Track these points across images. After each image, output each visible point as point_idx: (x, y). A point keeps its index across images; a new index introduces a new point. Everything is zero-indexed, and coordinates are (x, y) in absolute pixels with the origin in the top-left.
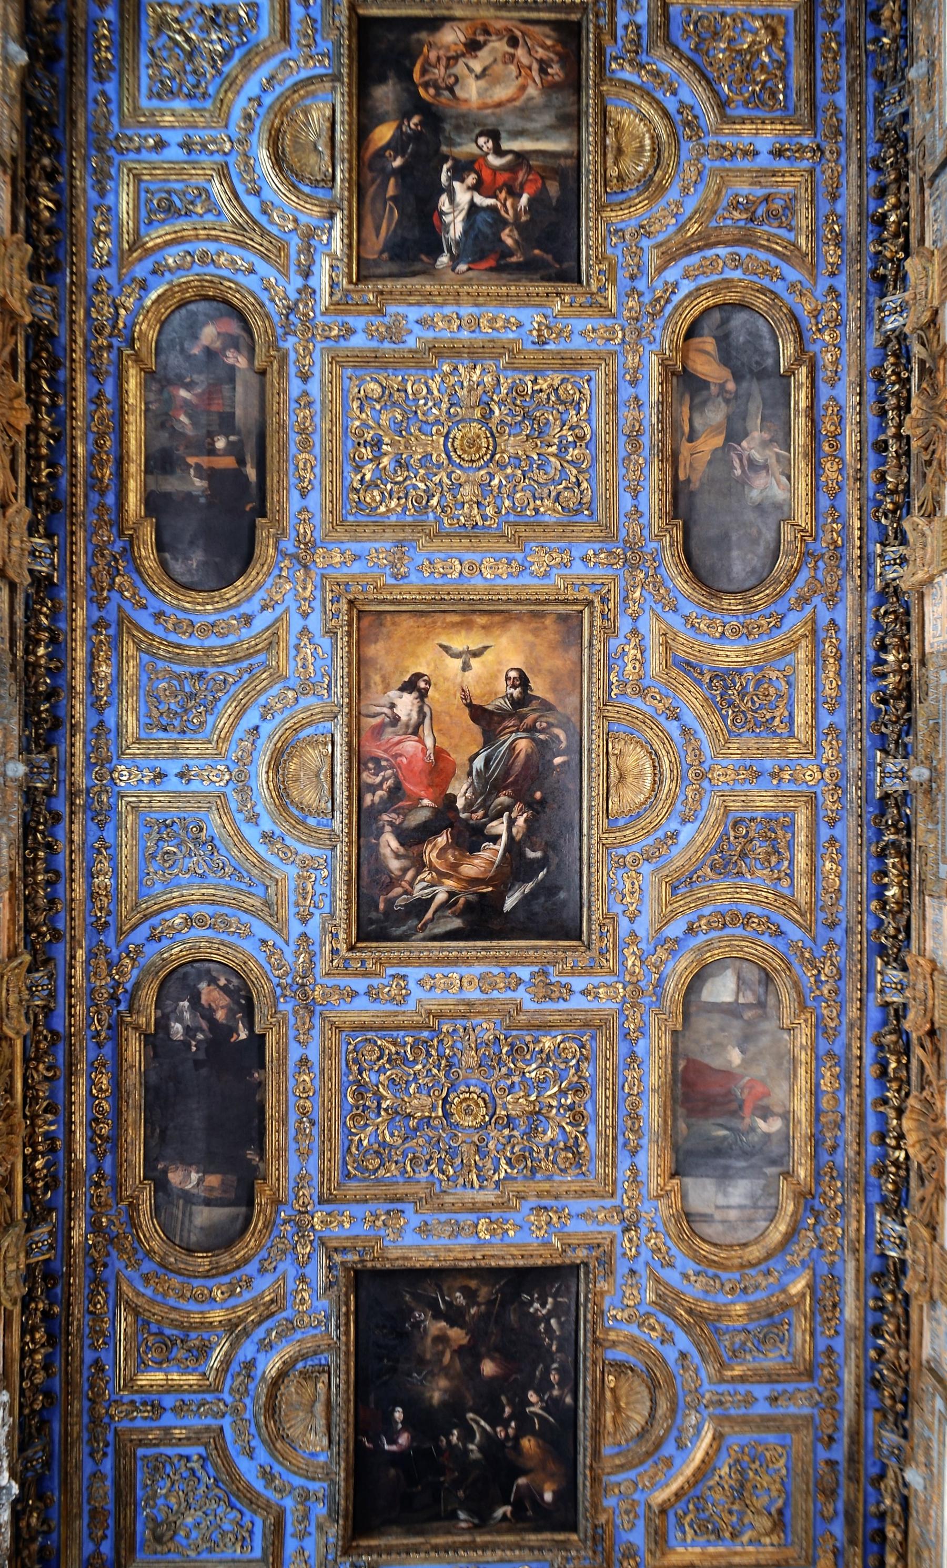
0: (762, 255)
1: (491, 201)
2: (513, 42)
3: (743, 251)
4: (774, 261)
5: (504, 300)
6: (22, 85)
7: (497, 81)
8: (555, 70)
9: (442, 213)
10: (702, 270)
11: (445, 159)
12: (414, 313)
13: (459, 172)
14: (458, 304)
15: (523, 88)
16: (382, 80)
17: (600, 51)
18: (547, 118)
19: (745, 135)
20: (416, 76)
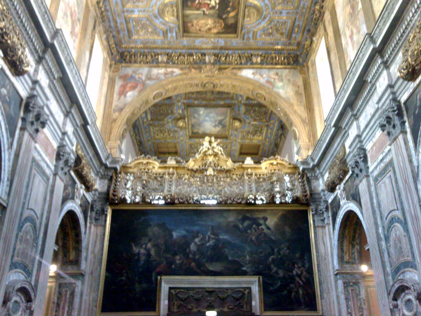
2: (200, 30)
6: (316, 32)
8: (189, 25)
11: (217, 10)
13: (213, 8)
15: (198, 22)
16: (232, 25)
17: (179, 28)
18: (191, 17)
19: (142, 15)
20: (223, 25)
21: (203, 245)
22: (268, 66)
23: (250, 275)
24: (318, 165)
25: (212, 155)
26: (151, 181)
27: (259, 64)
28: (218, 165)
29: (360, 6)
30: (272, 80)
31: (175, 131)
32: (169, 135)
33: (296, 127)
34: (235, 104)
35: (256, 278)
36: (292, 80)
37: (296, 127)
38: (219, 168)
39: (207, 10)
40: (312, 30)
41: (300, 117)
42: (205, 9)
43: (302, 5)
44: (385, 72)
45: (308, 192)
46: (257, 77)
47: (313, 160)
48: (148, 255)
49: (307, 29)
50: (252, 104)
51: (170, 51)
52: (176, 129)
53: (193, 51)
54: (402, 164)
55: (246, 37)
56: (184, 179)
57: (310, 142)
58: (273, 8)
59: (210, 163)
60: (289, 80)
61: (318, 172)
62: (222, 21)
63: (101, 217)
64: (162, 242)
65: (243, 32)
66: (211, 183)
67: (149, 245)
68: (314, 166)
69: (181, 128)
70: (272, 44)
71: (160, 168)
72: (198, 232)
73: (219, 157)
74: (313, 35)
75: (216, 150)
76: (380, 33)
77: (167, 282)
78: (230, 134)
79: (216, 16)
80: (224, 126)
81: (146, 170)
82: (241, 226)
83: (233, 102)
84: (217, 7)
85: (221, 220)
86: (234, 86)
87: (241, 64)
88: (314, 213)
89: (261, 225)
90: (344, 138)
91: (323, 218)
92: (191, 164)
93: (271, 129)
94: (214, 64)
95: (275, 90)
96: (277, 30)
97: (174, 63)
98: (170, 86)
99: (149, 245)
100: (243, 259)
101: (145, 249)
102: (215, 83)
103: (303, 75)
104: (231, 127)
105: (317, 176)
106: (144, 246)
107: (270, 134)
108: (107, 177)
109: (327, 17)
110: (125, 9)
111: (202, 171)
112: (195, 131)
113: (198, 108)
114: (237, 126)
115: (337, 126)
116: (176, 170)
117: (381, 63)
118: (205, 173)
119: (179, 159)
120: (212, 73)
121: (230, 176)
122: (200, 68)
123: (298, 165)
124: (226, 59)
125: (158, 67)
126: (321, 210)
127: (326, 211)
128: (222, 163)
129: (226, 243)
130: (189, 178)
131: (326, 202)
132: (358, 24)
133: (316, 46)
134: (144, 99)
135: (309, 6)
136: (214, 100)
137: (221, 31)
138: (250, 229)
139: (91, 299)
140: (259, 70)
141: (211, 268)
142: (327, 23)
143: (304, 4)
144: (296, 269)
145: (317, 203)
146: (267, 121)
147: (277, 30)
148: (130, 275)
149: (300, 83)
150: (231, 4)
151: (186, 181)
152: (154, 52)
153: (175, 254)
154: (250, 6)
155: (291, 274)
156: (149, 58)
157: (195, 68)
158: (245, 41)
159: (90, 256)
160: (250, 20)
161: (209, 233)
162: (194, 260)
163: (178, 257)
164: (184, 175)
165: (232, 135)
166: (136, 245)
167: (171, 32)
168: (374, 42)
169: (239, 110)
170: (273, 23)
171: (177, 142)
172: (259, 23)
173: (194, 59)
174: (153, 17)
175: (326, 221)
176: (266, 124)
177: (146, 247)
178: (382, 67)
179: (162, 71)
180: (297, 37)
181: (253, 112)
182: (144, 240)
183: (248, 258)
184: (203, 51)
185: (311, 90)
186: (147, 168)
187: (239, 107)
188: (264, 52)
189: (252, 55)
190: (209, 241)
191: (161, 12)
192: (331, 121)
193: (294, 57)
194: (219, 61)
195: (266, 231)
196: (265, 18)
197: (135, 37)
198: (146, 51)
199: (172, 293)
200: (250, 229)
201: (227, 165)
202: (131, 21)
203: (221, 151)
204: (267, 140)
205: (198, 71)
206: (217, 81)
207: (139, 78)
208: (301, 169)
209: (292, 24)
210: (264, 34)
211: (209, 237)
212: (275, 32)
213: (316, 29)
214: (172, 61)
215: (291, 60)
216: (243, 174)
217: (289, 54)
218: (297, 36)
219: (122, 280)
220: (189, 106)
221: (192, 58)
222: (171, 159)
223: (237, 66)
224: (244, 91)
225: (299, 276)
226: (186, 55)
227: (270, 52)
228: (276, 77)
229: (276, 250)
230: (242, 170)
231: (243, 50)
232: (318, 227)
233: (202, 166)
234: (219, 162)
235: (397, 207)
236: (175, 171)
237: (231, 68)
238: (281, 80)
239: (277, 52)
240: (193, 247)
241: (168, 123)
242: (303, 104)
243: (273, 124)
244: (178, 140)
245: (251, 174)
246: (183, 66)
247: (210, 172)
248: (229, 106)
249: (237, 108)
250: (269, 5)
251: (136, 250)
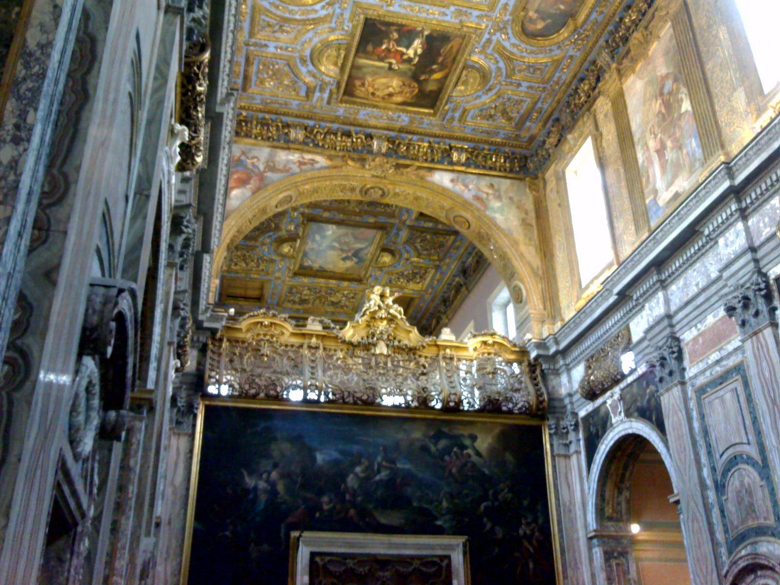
0: (279, 13)
1: (400, 49)
2: (373, 94)
3: (287, 15)
4: (273, 10)
5: (405, 17)
6: (573, 127)
7: (383, 84)
8: (358, 83)
9: (422, 48)
10: (308, 12)
11: (414, 65)
12: (448, 18)
13: (410, 60)
14: (426, 18)
15: (373, 81)
16: (431, 92)
18: (365, 70)
20: (417, 91)
21: (368, 478)
22: (477, 171)
23: (448, 534)
24: (564, 352)
25: (385, 318)
26: (277, 358)
27: (463, 165)
28: (395, 338)
29: (686, 106)
30: (485, 196)
31: (272, 261)
32: (258, 266)
33: (522, 281)
34: (393, 225)
35: (460, 540)
36: (515, 199)
37: (522, 281)
38: (396, 343)
39: (397, 63)
40: (565, 119)
41: (530, 265)
42: (394, 61)
43: (555, 79)
44: (740, 225)
45: (546, 397)
46: (459, 188)
47: (557, 342)
48: (273, 492)
49: (553, 117)
50: (423, 227)
51: (311, 123)
52: (274, 257)
53: (352, 129)
54: (767, 374)
55: (447, 117)
56: (335, 358)
57: (545, 309)
58: (508, 76)
59: (381, 333)
60: (511, 199)
61: (561, 362)
62: (416, 85)
63: (186, 420)
64: (298, 471)
65: (447, 107)
66: (383, 368)
67: (274, 475)
68: (557, 353)
69: (284, 256)
70: (488, 133)
71: (294, 334)
72: (361, 455)
73: (397, 324)
74: (570, 128)
75: (392, 311)
76: (746, 165)
77: (307, 544)
78: (367, 276)
79: (410, 74)
80: (361, 260)
81: (268, 337)
82: (433, 448)
83: (392, 221)
84: (417, 59)
85: (401, 436)
86: (417, 198)
87: (433, 161)
88: (552, 431)
89: (466, 447)
90: (631, 314)
91: (568, 442)
92: (348, 333)
93: (442, 273)
94: (385, 155)
95: (487, 213)
96: (504, 113)
97: (317, 145)
98: (307, 187)
99: (274, 475)
100: (437, 506)
101: (267, 481)
102: (386, 190)
103: (534, 193)
104: (373, 264)
105: (558, 370)
106: (264, 476)
107: (438, 281)
108: (196, 345)
109: (603, 106)
110: (253, 40)
111: (367, 347)
112: (306, 264)
113: (324, 225)
114: (384, 263)
115: (624, 296)
116: (322, 341)
117: (736, 211)
118: (373, 351)
119: (327, 321)
120: (383, 171)
121: (415, 358)
122: (363, 160)
123: (529, 349)
124: (408, 148)
125: (289, 149)
126: (564, 428)
127: (574, 430)
128: (401, 335)
129: (408, 477)
130: (344, 358)
131: (575, 414)
132: (678, 134)
133: (571, 150)
134: (261, 207)
135: (567, 81)
136: (358, 214)
137: (409, 101)
138: (449, 454)
139: (169, 573)
140: (462, 176)
142: (600, 117)
143: (560, 78)
145: (557, 415)
146: (438, 260)
147: (504, 113)
148: (239, 528)
149: (530, 206)
150: (440, 59)
151: (339, 362)
152: (281, 122)
153: (320, 493)
154: (473, 67)
155: (515, 534)
156: (273, 130)
157: (353, 159)
158: (444, 122)
159: (169, 490)
160: (466, 89)
161: (379, 459)
162: (354, 505)
163: (325, 499)
164: (335, 350)
165: (371, 276)
166: (251, 473)
167: (322, 90)
168: (732, 177)
169: (397, 234)
170: (501, 100)
171: (270, 281)
172: (479, 97)
173: (353, 142)
174: (298, 61)
175: (573, 448)
176: (437, 263)
178: (736, 216)
179: (295, 157)
180: (533, 127)
181: (422, 241)
183: (445, 504)
184: (369, 131)
185: (548, 221)
186: (269, 333)
187: (399, 229)
188: (472, 145)
189: (451, 148)
190: (379, 472)
191: (316, 55)
192: (615, 285)
193: (521, 158)
194: (396, 152)
195: (475, 458)
196: (490, 90)
197: (253, 89)
198: (267, 116)
199: (316, 563)
200: (449, 454)
201: (409, 340)
202: (256, 62)
203: (400, 313)
204: (430, 290)
205: (358, 165)
206: (390, 187)
207: (253, 164)
208: (533, 354)
209: (530, 106)
210: (480, 116)
211: (380, 465)
212: (499, 114)
213: (575, 121)
214: (313, 141)
215: (517, 164)
216: (438, 355)
217: (513, 153)
218: (533, 125)
220: (312, 219)
221: (350, 140)
222: (313, 321)
223: (426, 165)
224: (435, 208)
225: (529, 538)
226: (339, 134)
227: (481, 146)
228: (490, 191)
229: (491, 492)
230: (434, 349)
231: (438, 137)
232: (559, 455)
233: (368, 337)
234: (398, 333)
235: (748, 439)
236: (319, 342)
237: (415, 168)
238: (499, 198)
239: (493, 148)
240: (351, 481)
241: (263, 244)
242: (533, 243)
243: (448, 265)
244: (269, 277)
245: (451, 359)
246: (333, 152)
247: (382, 349)
248: (381, 227)
249: (394, 231)
250: (504, 71)
251: (250, 482)
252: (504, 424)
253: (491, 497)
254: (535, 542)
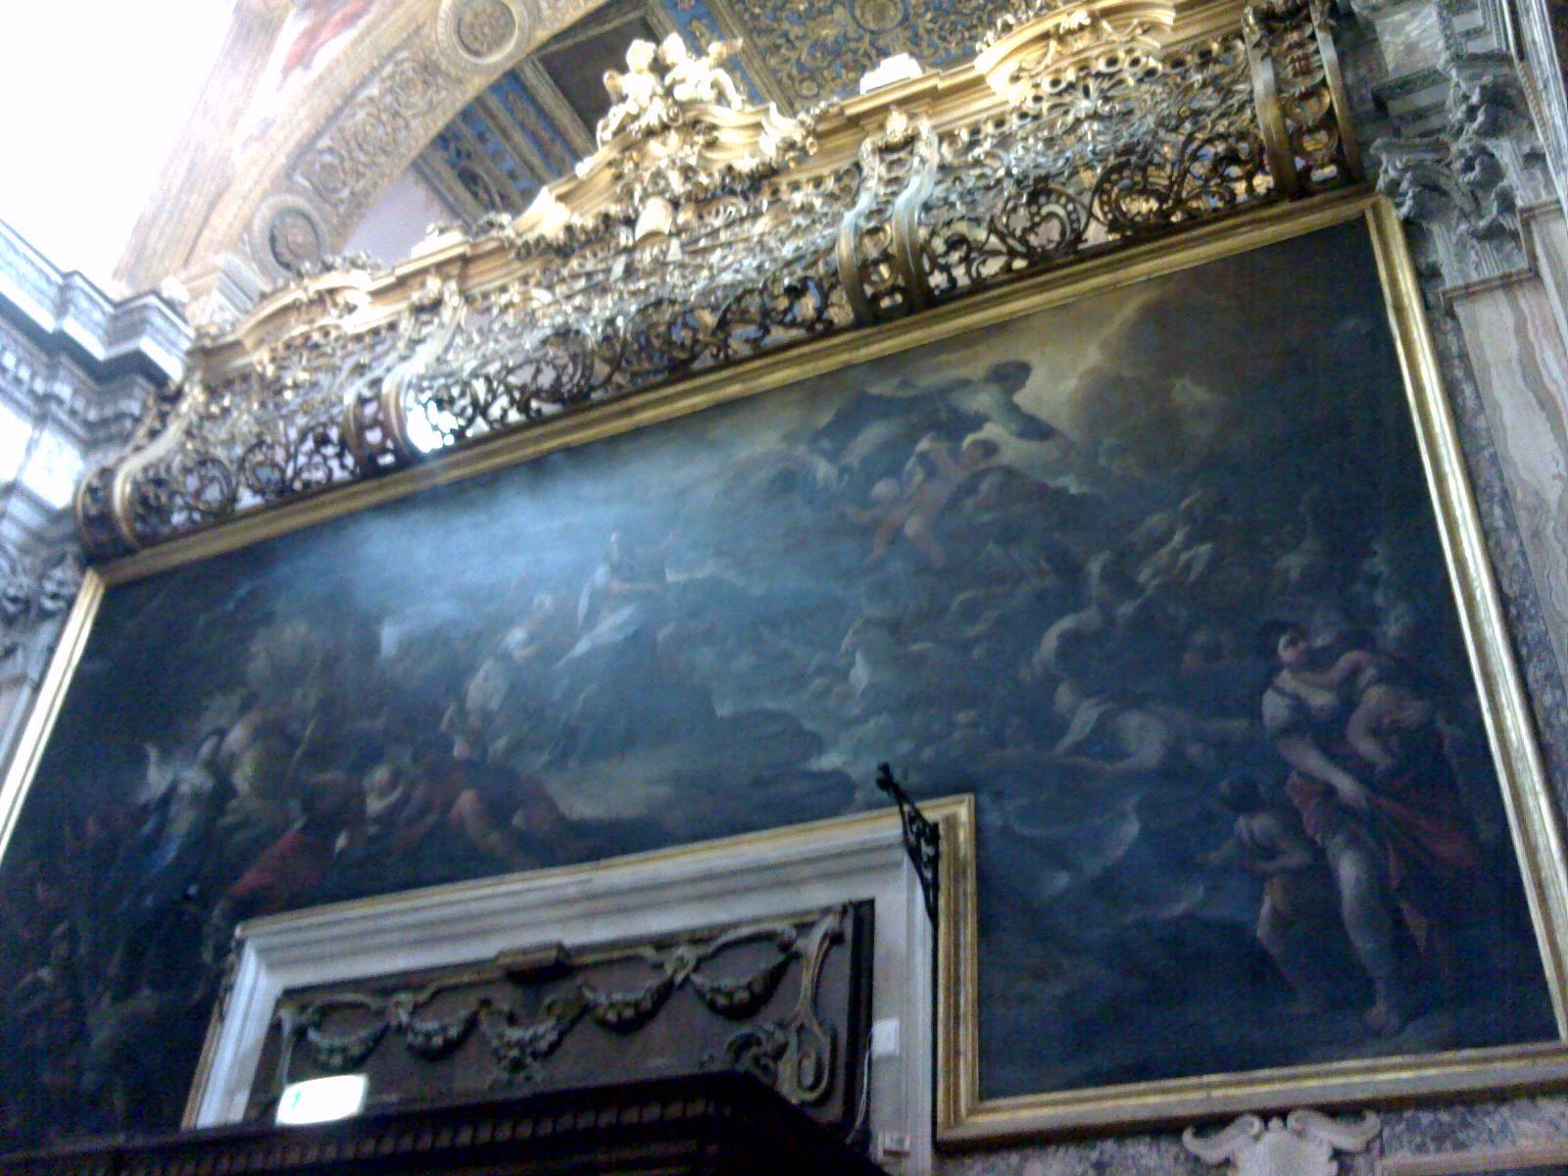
25: (665, 127)
67: (237, 736)
77: (272, 960)
89: (976, 422)
100: (826, 691)
141: (583, 803)
144: (1285, 679)
155: (1237, 725)
166: (166, 754)
177: (217, 748)
182: (219, 707)
183: (861, 674)
195: (1014, 450)
200: (894, 471)
219: (37, 986)
225: (1327, 732)
229: (1095, 567)
247: (654, 216)
252: (1149, 281)
253: (1095, 587)
254: (1366, 747)
